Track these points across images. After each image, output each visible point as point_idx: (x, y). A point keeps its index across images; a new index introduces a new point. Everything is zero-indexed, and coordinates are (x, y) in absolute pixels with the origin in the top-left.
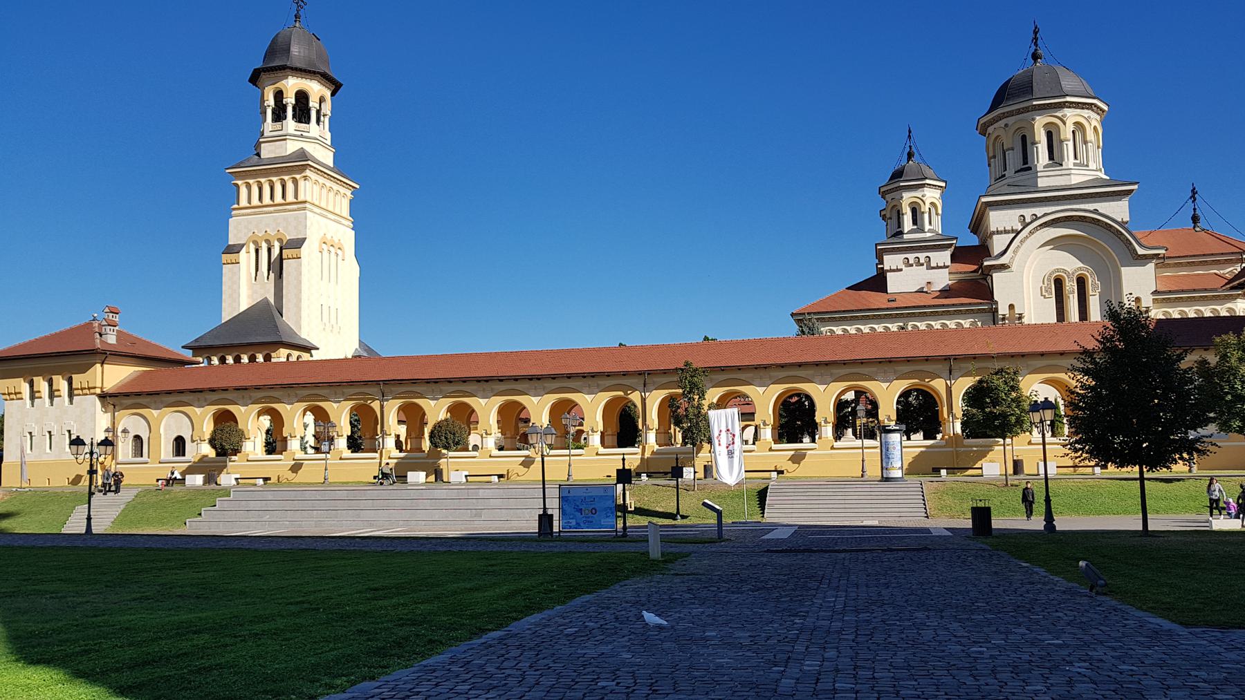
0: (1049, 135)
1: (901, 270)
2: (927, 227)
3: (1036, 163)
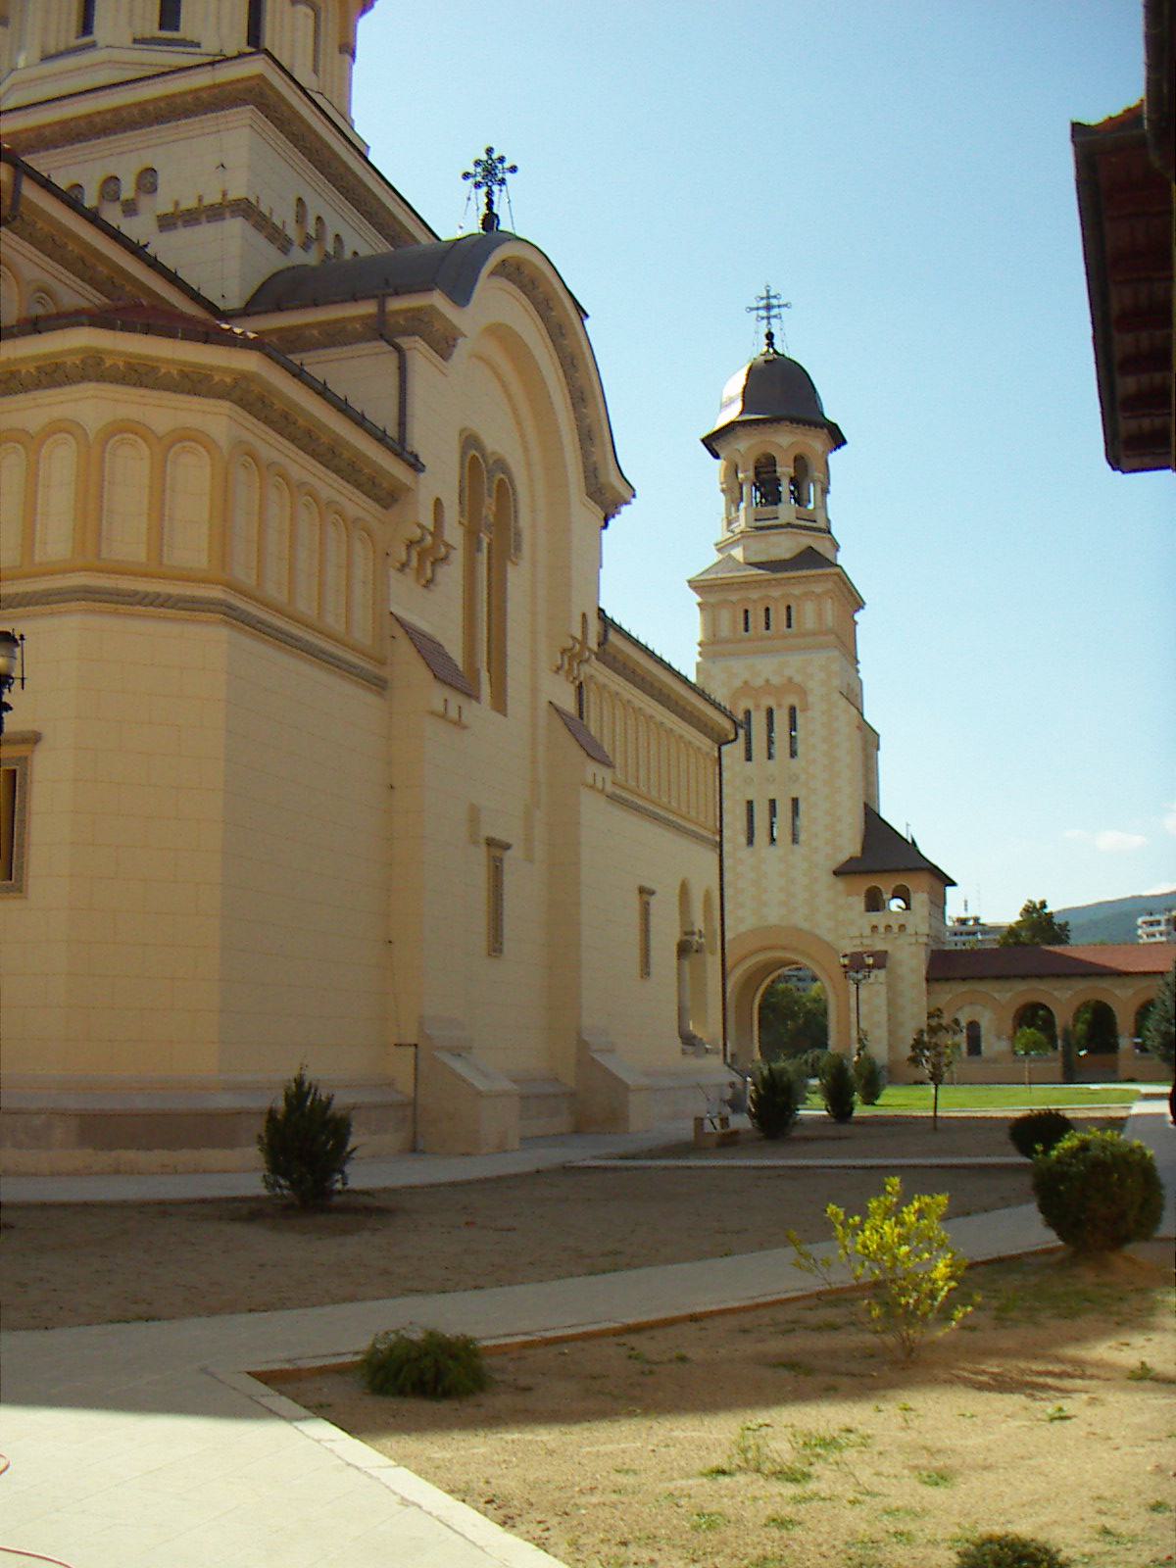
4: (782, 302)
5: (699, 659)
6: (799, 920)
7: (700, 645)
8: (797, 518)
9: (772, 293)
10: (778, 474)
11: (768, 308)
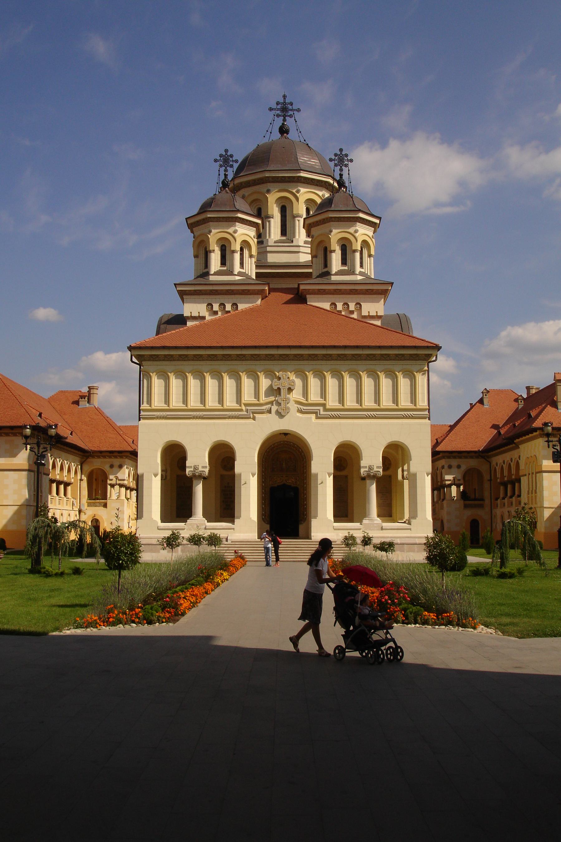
0: (283, 210)
1: (204, 318)
2: (237, 268)
3: (268, 238)
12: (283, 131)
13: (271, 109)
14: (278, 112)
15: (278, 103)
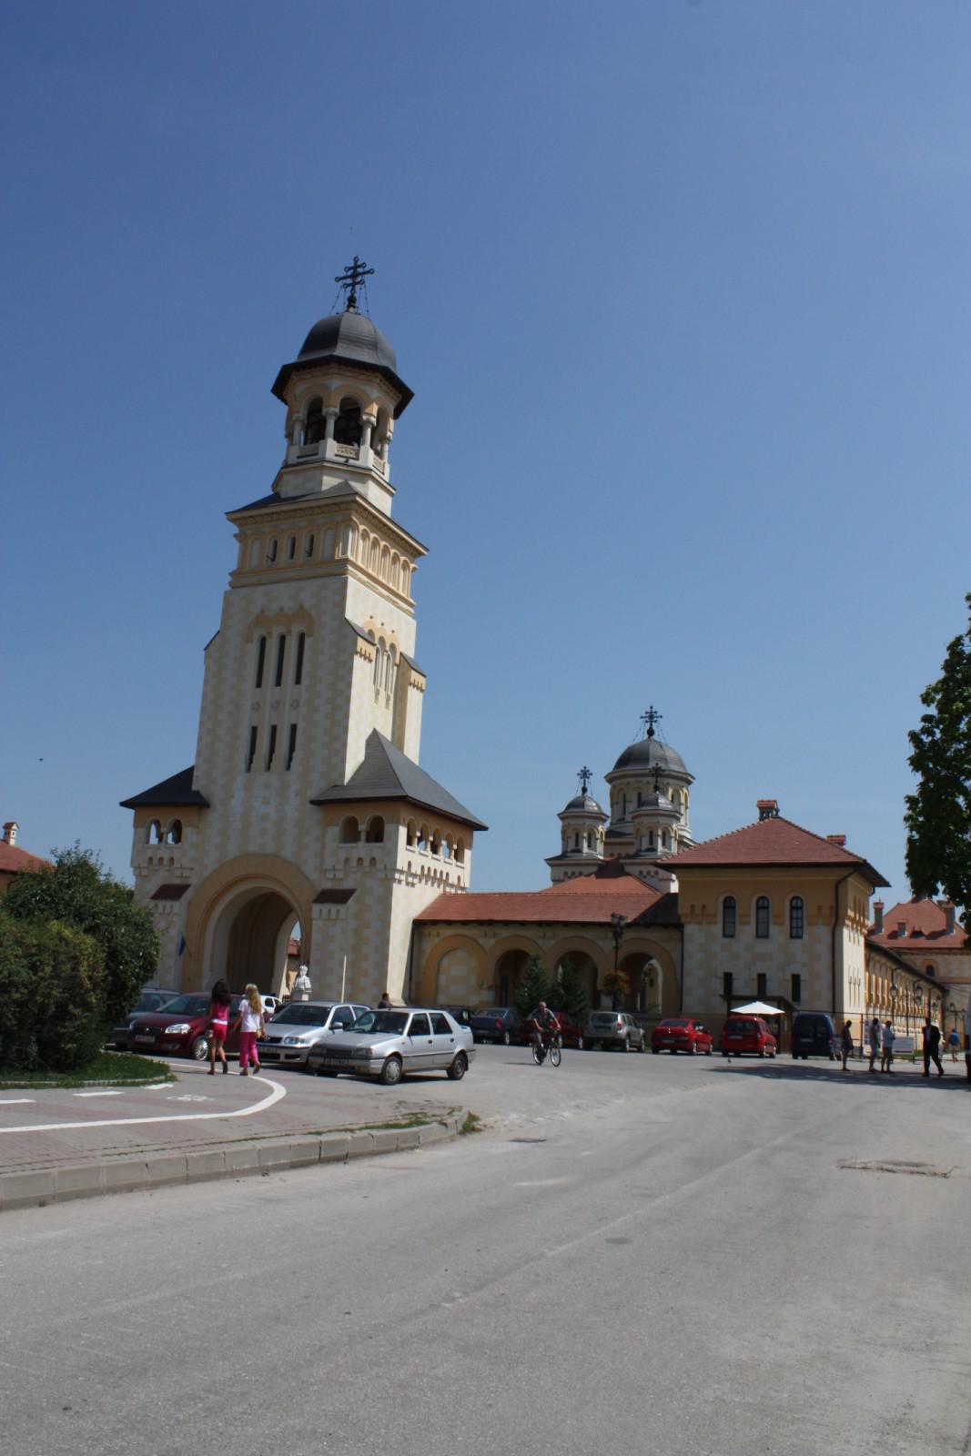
4: (366, 269)
5: (228, 588)
6: (288, 853)
7: (231, 574)
8: (337, 455)
9: (359, 263)
10: (323, 414)
11: (354, 276)
12: (651, 732)
13: (642, 717)
14: (647, 719)
15: (647, 713)
